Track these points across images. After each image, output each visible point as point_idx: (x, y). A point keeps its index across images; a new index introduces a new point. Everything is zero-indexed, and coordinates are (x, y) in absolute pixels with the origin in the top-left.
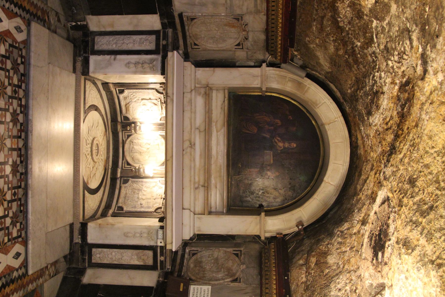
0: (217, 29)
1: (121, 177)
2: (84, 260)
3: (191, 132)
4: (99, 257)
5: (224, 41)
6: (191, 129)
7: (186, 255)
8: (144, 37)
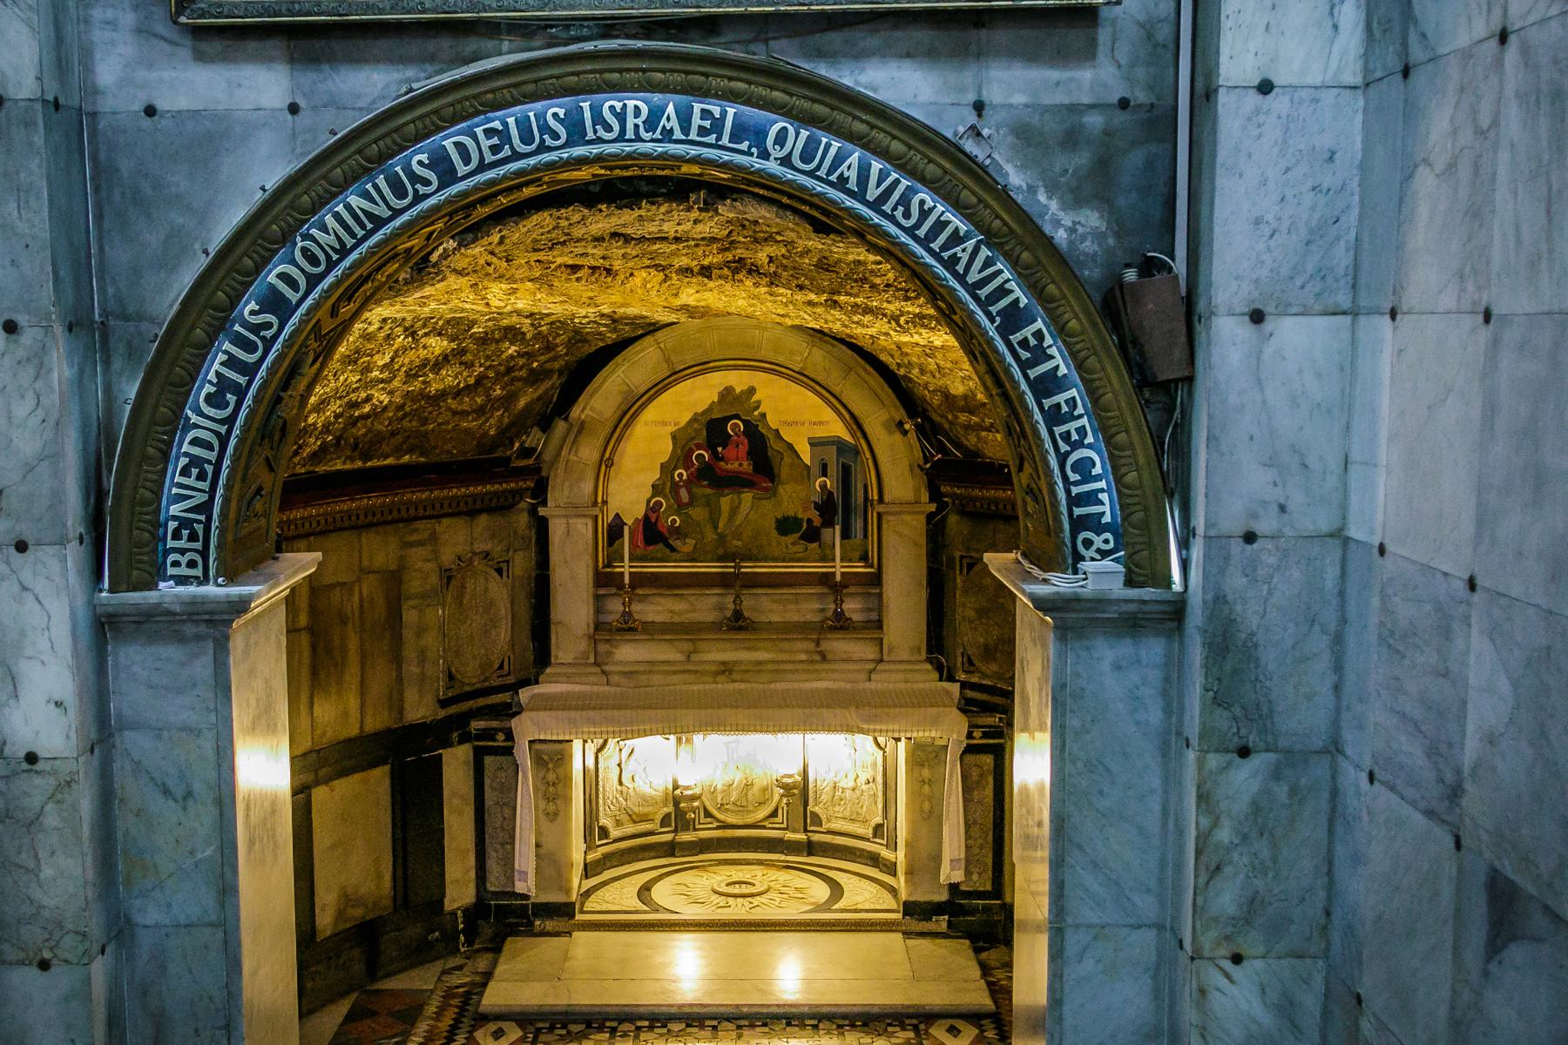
0: (469, 622)
2: (986, 909)
3: (696, 672)
4: (980, 874)
5: (492, 603)
6: (689, 672)
7: (973, 680)
8: (487, 782)
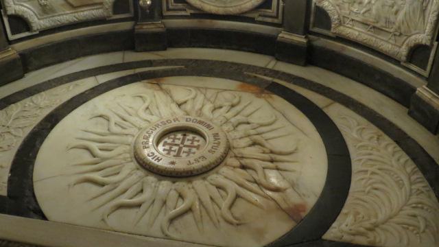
1: (306, 32)
